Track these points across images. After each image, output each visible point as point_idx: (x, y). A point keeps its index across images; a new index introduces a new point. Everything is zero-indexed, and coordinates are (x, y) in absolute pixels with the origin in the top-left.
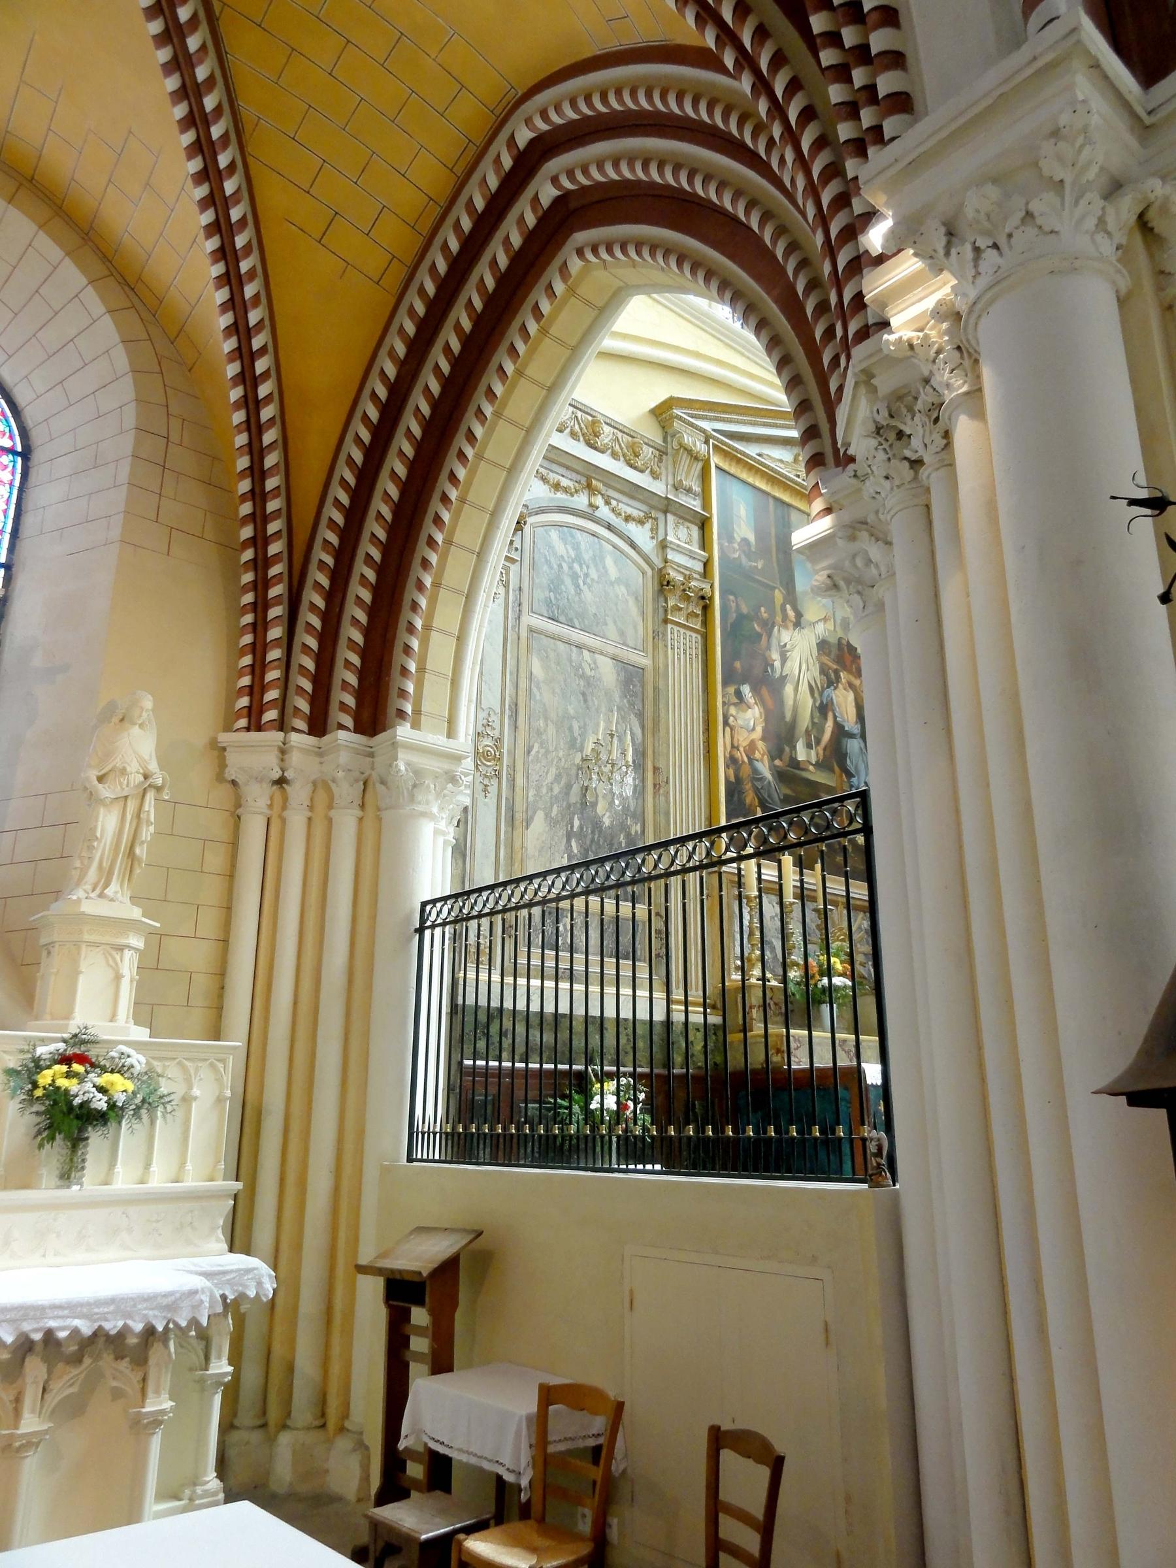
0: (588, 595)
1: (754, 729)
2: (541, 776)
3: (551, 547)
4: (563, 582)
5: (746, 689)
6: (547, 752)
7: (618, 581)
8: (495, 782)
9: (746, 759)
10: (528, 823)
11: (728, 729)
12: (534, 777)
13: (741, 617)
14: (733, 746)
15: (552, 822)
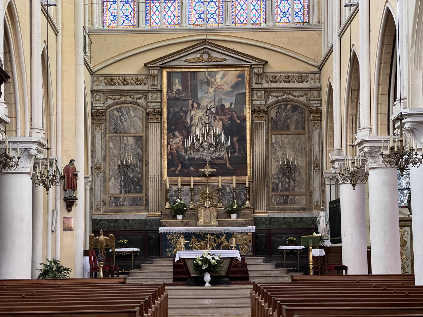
0: (125, 123)
1: (179, 143)
2: (112, 169)
3: (114, 115)
4: (118, 122)
5: (176, 133)
6: (115, 163)
7: (134, 116)
8: (100, 174)
9: (175, 152)
10: (110, 180)
11: (169, 146)
12: (111, 170)
13: (175, 113)
14: (171, 149)
15: (116, 179)
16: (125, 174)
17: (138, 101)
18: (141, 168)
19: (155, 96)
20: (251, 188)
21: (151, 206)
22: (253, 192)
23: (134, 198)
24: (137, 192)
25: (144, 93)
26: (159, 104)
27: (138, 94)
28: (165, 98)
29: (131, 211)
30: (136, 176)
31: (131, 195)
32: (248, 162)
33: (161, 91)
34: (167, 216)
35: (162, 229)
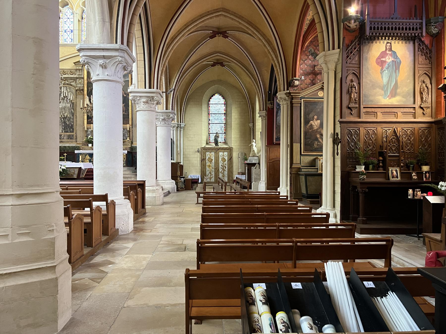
16: (65, 122)
17: (72, 83)
18: (73, 119)
19: (80, 81)
20: (131, 130)
21: (78, 140)
22: (132, 132)
23: (69, 135)
24: (71, 132)
25: (75, 79)
26: (82, 85)
27: (71, 80)
28: (86, 82)
29: (68, 142)
30: (71, 124)
31: (68, 134)
32: (130, 117)
33: (83, 78)
34: (83, 144)
35: (76, 152)
